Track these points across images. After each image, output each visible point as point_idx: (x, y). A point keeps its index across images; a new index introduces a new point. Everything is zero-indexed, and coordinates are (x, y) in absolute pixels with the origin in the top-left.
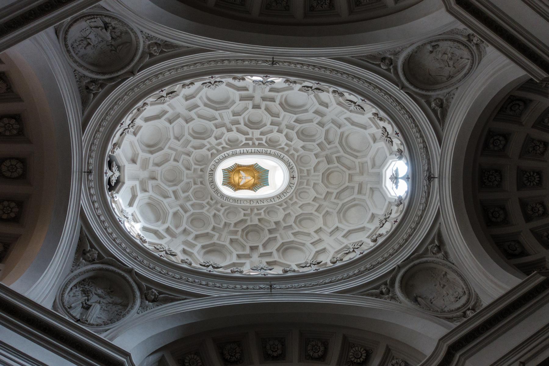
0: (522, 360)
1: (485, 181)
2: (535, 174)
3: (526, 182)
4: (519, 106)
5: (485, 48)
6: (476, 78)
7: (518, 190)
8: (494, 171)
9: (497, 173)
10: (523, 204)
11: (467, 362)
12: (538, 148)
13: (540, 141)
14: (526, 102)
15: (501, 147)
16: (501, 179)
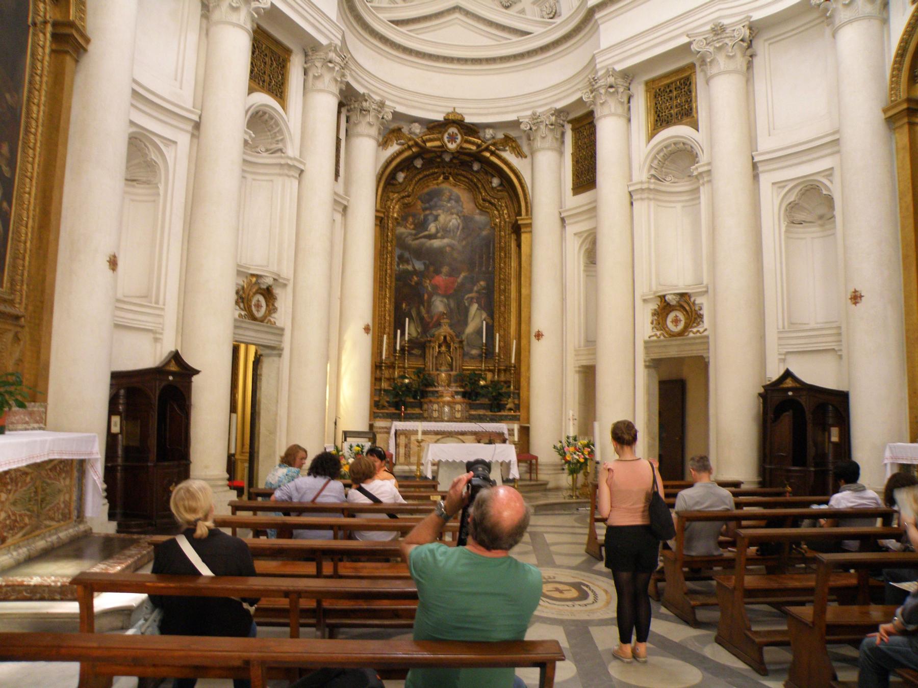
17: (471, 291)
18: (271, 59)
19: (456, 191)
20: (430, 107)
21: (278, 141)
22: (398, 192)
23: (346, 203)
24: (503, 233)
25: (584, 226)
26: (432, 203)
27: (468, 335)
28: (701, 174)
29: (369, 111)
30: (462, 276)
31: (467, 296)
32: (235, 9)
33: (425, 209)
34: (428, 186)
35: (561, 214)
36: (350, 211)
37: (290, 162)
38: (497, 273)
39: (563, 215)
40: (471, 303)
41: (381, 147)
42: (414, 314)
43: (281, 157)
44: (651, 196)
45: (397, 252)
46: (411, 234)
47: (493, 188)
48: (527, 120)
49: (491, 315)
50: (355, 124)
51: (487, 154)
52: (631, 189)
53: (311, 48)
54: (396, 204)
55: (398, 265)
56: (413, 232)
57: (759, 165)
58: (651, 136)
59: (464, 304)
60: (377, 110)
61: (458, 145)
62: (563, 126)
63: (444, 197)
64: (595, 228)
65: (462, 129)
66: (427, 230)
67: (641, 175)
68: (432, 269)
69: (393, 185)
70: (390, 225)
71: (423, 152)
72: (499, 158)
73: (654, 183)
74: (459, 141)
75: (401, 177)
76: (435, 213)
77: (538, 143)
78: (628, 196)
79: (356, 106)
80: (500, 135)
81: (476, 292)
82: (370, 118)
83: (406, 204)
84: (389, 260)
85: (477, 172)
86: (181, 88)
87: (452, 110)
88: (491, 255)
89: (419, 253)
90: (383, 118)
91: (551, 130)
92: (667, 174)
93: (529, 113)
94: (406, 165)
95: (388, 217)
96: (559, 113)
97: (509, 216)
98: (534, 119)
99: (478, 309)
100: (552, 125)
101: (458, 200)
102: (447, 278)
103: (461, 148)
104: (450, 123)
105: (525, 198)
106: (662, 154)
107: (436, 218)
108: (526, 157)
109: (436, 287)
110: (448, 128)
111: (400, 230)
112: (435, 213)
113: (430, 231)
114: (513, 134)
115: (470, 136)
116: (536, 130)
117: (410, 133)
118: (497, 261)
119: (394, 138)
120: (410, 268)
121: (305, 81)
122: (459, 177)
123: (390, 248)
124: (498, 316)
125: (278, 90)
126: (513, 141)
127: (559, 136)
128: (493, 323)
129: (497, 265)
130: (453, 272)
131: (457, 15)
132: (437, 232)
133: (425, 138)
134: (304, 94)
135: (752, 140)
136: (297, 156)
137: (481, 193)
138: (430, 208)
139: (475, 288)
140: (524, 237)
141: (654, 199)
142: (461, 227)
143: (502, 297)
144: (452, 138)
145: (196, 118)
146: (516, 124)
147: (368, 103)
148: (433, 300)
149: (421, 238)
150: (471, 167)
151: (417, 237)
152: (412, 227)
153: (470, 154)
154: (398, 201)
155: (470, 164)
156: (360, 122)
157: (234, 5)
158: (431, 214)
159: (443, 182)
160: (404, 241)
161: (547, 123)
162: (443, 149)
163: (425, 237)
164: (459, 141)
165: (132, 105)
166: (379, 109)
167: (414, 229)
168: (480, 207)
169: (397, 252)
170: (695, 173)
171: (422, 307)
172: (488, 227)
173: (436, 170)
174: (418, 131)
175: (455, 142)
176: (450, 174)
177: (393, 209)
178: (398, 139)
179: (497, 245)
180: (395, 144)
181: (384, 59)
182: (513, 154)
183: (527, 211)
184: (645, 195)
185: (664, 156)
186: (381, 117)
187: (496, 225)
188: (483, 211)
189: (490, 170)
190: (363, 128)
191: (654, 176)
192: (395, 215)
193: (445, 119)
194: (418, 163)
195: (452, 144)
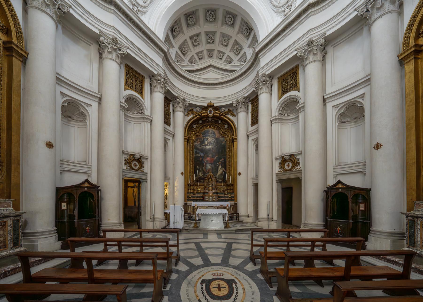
0: (130, 47)
1: (209, 12)
2: (213, 41)
3: (209, 36)
4: (247, 33)
5: (281, 16)
6: (267, 9)
7: (205, 32)
8: (215, 17)
9: (213, 19)
10: (198, 35)
11: (113, 15)
12: (225, 42)
13: (228, 43)
14: (248, 37)
15: (227, 22)
16: (211, 22)
17: (219, 162)
18: (135, 79)
19: (213, 130)
21: (141, 109)
22: (194, 132)
23: (174, 134)
25: (254, 137)
26: (206, 135)
28: (300, 108)
29: (180, 102)
30: (216, 157)
32: (110, 52)
33: (203, 137)
34: (204, 129)
36: (175, 136)
37: (146, 116)
39: (248, 134)
41: (186, 116)
43: (142, 115)
44: (279, 121)
45: (195, 150)
46: (199, 145)
47: (226, 129)
48: (235, 102)
50: (176, 107)
51: (223, 117)
52: (271, 119)
53: (152, 76)
54: (193, 135)
55: (195, 155)
56: (200, 144)
57: (326, 100)
58: (279, 99)
60: (183, 102)
62: (248, 103)
64: (258, 137)
67: (275, 113)
68: (206, 155)
69: (193, 129)
70: (192, 142)
71: (201, 118)
72: (227, 117)
73: (281, 116)
74: (213, 113)
75: (195, 126)
76: (207, 138)
77: (239, 110)
78: (270, 122)
79: (175, 101)
80: (227, 110)
82: (181, 105)
83: (197, 135)
84: (192, 153)
85: (220, 124)
86: (92, 85)
87: (210, 102)
89: (202, 151)
90: (185, 105)
91: (244, 105)
92: (286, 113)
94: (196, 122)
95: (191, 139)
96: (246, 98)
97: (231, 137)
100: (243, 103)
101: (214, 133)
103: (214, 115)
104: (209, 107)
105: (235, 130)
106: (284, 105)
108: (235, 116)
109: (207, 161)
111: (195, 144)
112: (207, 138)
114: (231, 109)
116: (238, 105)
117: (197, 111)
118: (227, 152)
119: (191, 113)
120: (199, 155)
121: (151, 89)
122: (214, 126)
123: (192, 149)
125: (141, 91)
126: (231, 111)
127: (246, 107)
129: (227, 153)
130: (213, 156)
131: (211, 68)
134: (151, 93)
135: (324, 88)
136: (149, 114)
137: (221, 130)
138: (205, 136)
140: (235, 143)
141: (280, 122)
144: (211, 112)
145: (100, 96)
146: (231, 105)
147: (179, 99)
149: (202, 146)
150: (218, 122)
152: (199, 142)
153: (217, 117)
156: (177, 107)
157: (109, 50)
158: (206, 138)
159: (209, 128)
161: (242, 102)
163: (204, 145)
164: (213, 113)
165: (57, 83)
167: (200, 143)
169: (195, 150)
170: (297, 108)
174: (199, 110)
175: (212, 113)
176: (211, 125)
177: (193, 137)
178: (192, 113)
179: (227, 147)
180: (191, 115)
181: (185, 85)
183: (236, 134)
184: (277, 121)
185: (285, 105)
186: (184, 104)
188: (223, 136)
189: (224, 123)
190: (178, 109)
191: (280, 114)
192: (193, 139)
193: (208, 105)
194: (201, 122)
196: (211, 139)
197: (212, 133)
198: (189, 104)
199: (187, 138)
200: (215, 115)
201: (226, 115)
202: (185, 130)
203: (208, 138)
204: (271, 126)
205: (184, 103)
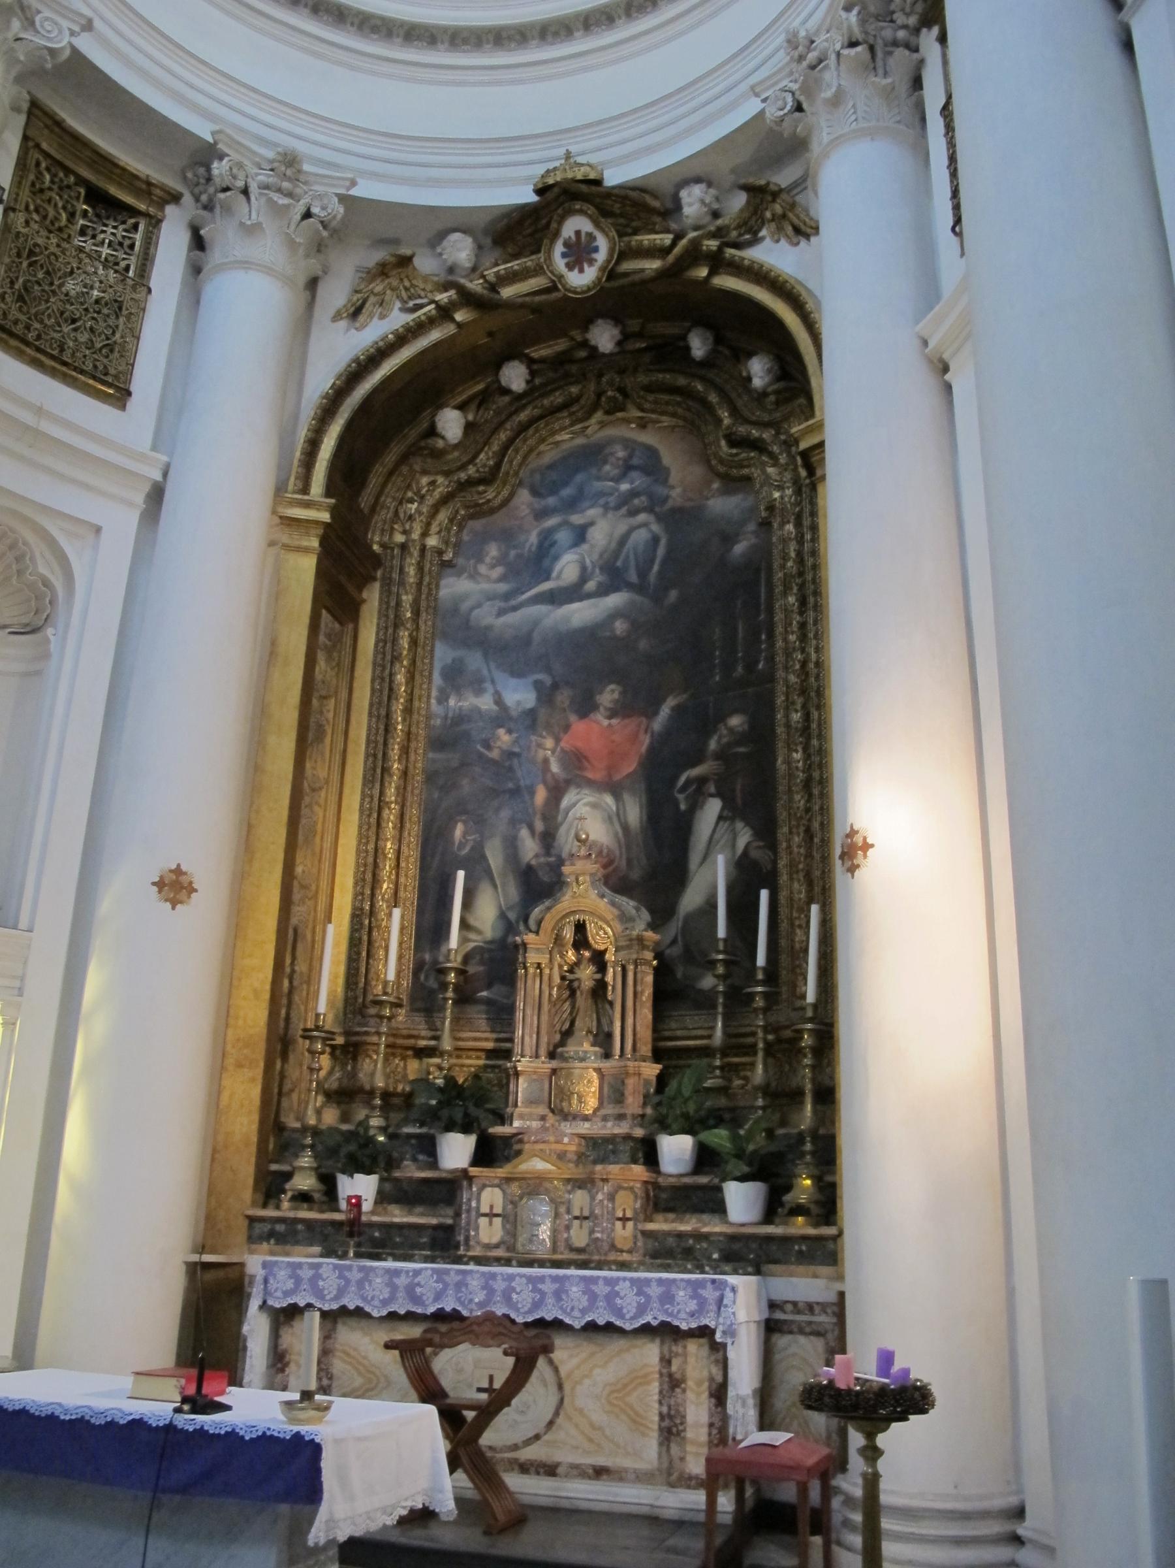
19: (647, 438)
20: (492, 173)
24: (790, 527)
27: (689, 918)
29: (245, 192)
30: (665, 711)
31: (683, 779)
33: (541, 514)
35: (925, 343)
38: (780, 674)
40: (695, 805)
41: (343, 324)
42: (495, 857)
45: (443, 654)
46: (491, 597)
49: (766, 831)
54: (436, 509)
56: (503, 587)
59: (676, 804)
61: (602, 269)
63: (607, 468)
65: (605, 213)
66: (548, 578)
69: (437, 454)
76: (577, 519)
81: (720, 756)
85: (705, 363)
88: (762, 617)
93: (782, 57)
98: (801, 58)
99: (720, 818)
100: (853, 44)
101: (653, 467)
102: (614, 721)
107: (581, 535)
110: (560, 223)
112: (577, 519)
113: (558, 577)
115: (636, 232)
117: (451, 270)
120: (485, 703)
124: (785, 829)
128: (775, 862)
132: (584, 578)
133: (490, 274)
137: (719, 421)
139: (713, 745)
142: (663, 542)
143: (798, 756)
144: (579, 253)
148: (565, 802)
150: (688, 349)
151: (513, 602)
152: (499, 571)
154: (445, 500)
155: (682, 344)
160: (468, 621)
162: (555, 295)
164: (601, 256)
166: (286, 185)
167: (503, 579)
168: (722, 469)
171: (524, 833)
172: (751, 527)
173: (574, 390)
182: (783, 242)
187: (771, 508)
188: (735, 482)
192: (432, 541)
193: (540, 191)
194: (515, 376)
195: (581, 271)
196: (622, 528)
197: (627, 468)
198: (343, 199)
199: (325, 517)
200: (626, 274)
201: (730, 252)
202: (313, 445)
203: (592, 524)
204: (1113, 56)
205: (290, 195)
